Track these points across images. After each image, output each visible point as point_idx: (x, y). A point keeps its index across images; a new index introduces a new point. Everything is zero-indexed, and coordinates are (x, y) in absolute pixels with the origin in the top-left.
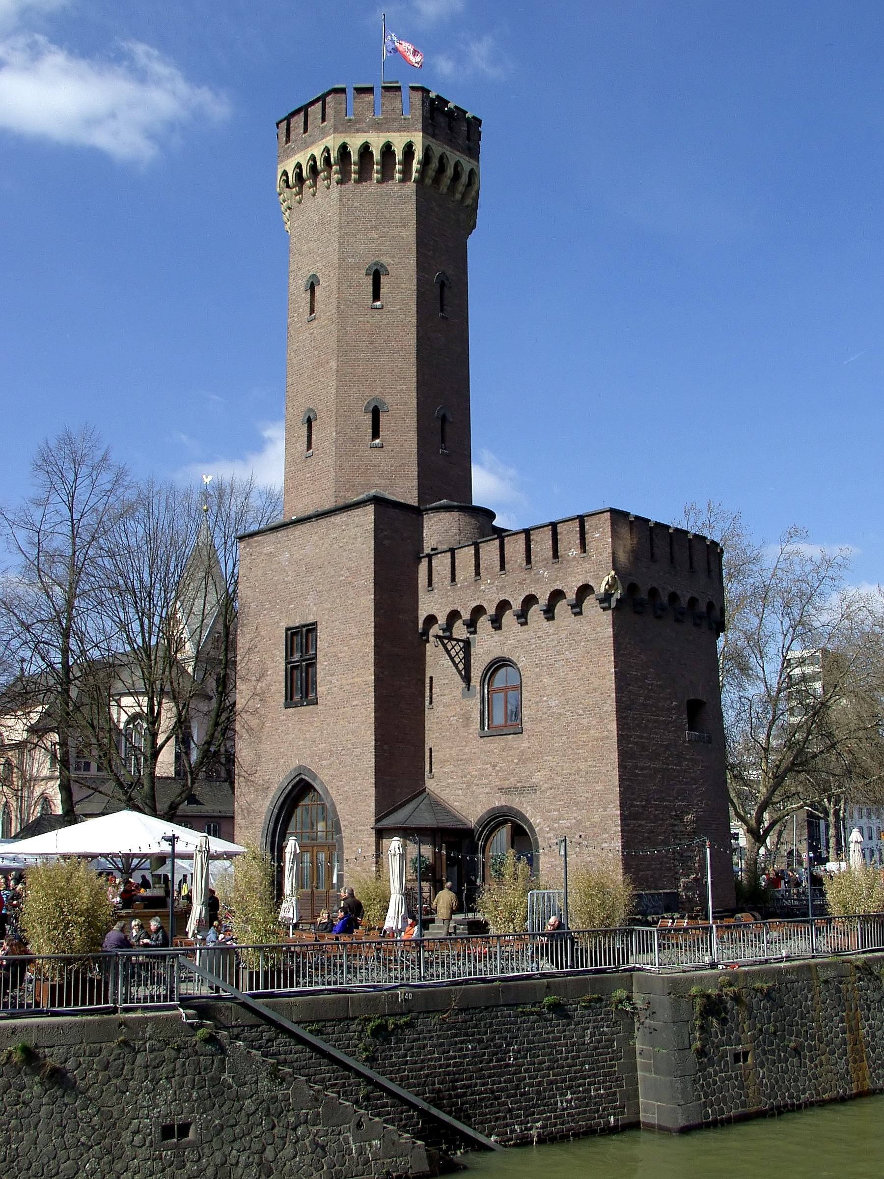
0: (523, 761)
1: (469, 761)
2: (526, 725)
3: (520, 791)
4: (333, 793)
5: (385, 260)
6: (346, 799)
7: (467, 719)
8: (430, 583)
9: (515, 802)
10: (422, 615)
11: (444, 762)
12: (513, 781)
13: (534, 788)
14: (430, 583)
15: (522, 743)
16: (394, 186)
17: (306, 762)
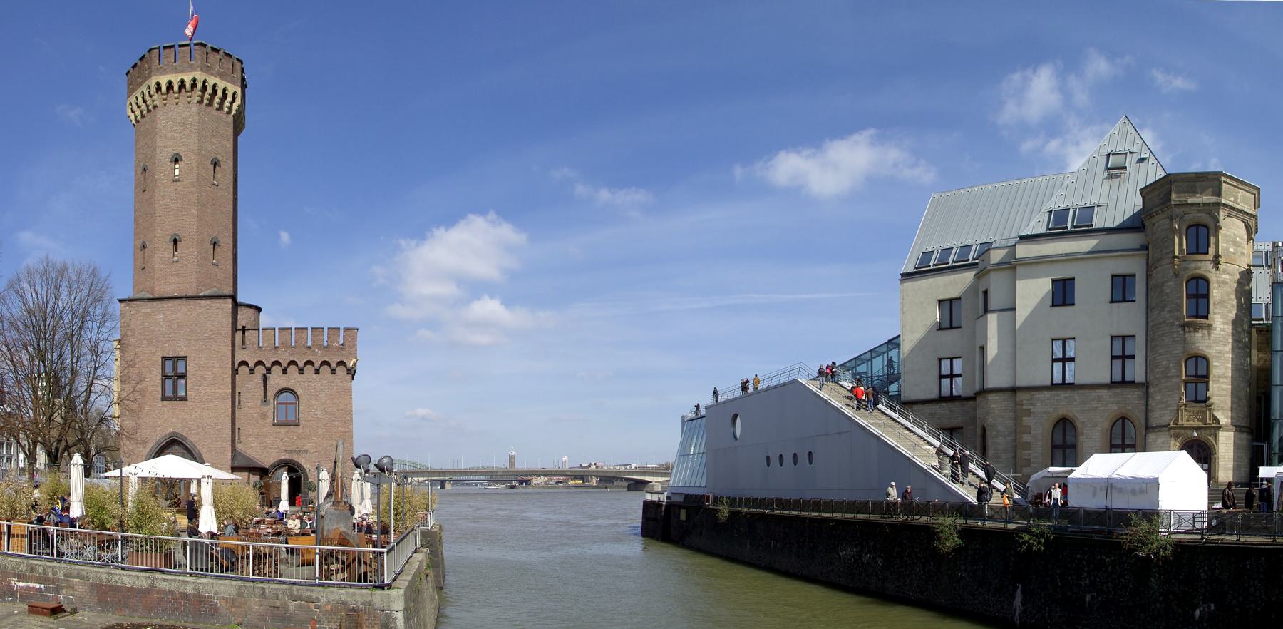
0: (299, 437)
1: (265, 436)
2: (302, 422)
3: (298, 452)
4: (200, 448)
5: (220, 158)
6: (210, 451)
7: (264, 416)
8: (243, 343)
9: (295, 457)
10: (238, 360)
11: (248, 436)
12: (293, 447)
13: (306, 451)
14: (243, 343)
15: (300, 430)
16: (223, 114)
17: (179, 431)
